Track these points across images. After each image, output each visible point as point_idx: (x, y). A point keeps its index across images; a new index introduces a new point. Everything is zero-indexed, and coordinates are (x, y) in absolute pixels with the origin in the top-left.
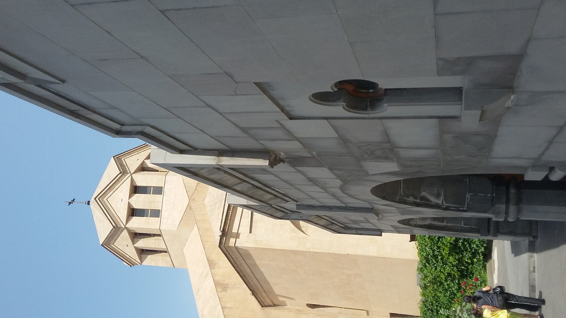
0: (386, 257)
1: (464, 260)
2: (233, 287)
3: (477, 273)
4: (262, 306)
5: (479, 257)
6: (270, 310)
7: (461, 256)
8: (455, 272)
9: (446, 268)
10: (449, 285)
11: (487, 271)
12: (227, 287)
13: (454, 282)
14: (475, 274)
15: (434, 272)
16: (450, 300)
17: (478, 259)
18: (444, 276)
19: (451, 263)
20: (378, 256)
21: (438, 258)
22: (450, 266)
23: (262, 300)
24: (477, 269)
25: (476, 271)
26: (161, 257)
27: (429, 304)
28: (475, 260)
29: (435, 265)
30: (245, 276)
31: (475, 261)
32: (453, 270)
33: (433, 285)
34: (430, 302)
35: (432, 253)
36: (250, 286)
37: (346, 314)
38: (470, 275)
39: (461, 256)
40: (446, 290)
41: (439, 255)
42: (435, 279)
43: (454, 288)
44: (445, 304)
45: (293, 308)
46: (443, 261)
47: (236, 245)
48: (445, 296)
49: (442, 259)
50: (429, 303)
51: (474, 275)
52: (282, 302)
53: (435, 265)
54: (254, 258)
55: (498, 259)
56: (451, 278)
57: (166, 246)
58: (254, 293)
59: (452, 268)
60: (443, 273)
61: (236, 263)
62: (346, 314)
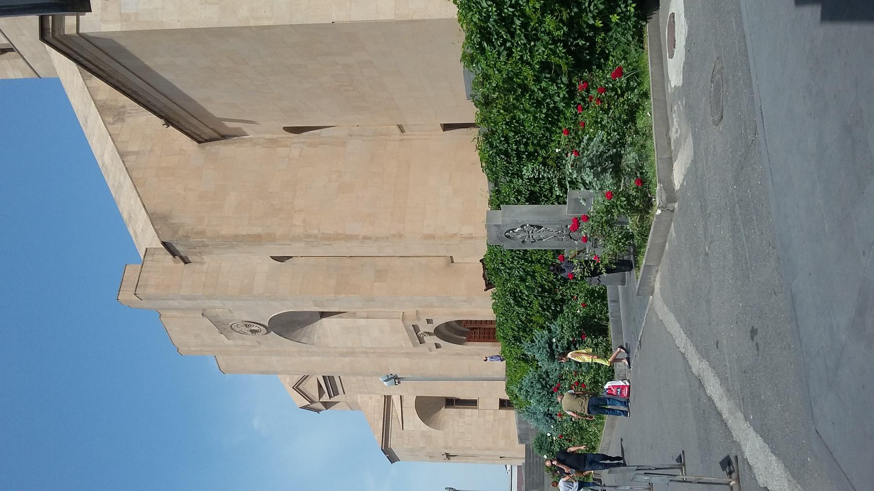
0: (415, 18)
1: (585, 22)
2: (137, 110)
3: (618, 53)
4: (199, 142)
5: (626, 7)
6: (216, 146)
7: (575, 10)
8: (561, 58)
9: (537, 51)
10: (547, 91)
11: (647, 46)
12: (124, 113)
13: (559, 81)
14: (613, 56)
15: (506, 63)
16: (549, 126)
17: (622, 12)
18: (531, 72)
19: (549, 33)
20: (396, 19)
21: (514, 23)
22: (548, 43)
23: (194, 130)
24: (619, 42)
25: (614, 49)
26: (6, 60)
27: (498, 141)
28: (615, 18)
29: (508, 44)
30: (135, 92)
31: (613, 20)
32: (554, 53)
33: (505, 95)
34: (501, 135)
35: (495, 11)
36: (156, 110)
37: (362, 135)
38: (600, 60)
39: (575, 10)
40: (539, 104)
41: (515, 16)
42: (509, 79)
43: (559, 96)
44: (536, 137)
45: (260, 138)
46: (526, 30)
47: (81, 31)
48: (535, 118)
49: (524, 26)
50: (499, 138)
51: (611, 58)
52: (236, 129)
53: (508, 44)
54: (137, 54)
55: (685, 12)
56: (550, 73)
57: (7, 38)
58: (169, 122)
59: (552, 47)
60: (528, 63)
61: (102, 70)
62: (362, 135)
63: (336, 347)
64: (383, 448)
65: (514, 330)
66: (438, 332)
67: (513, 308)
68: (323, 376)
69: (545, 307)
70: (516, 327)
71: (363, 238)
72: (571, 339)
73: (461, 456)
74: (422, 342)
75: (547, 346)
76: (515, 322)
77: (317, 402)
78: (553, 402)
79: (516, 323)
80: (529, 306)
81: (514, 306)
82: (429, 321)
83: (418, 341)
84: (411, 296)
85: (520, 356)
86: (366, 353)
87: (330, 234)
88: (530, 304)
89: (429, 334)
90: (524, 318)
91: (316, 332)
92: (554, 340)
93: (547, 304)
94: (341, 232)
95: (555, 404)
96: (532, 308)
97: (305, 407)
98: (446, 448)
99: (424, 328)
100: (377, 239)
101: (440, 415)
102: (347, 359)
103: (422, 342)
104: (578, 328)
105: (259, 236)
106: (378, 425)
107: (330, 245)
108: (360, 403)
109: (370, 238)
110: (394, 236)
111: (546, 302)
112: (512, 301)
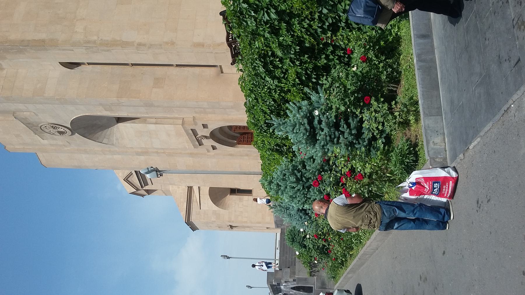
63: (132, 148)
64: (186, 222)
65: (265, 113)
66: (213, 135)
67: (264, 80)
68: (135, 171)
69: (304, 78)
70: (268, 108)
71: (138, 45)
72: (343, 108)
73: (240, 227)
74: (200, 144)
75: (306, 121)
76: (266, 102)
77: (141, 190)
78: (310, 198)
79: (268, 103)
80: (284, 77)
81: (265, 77)
82: (205, 126)
83: (197, 143)
84: (185, 101)
85: (273, 147)
86: (157, 153)
87: (108, 40)
88: (285, 74)
89: (206, 137)
90: (277, 96)
91: (114, 135)
92: (317, 113)
93: (306, 74)
94: (119, 39)
95: (311, 201)
96: (286, 79)
97: (133, 193)
98: (229, 222)
99: (201, 132)
100: (151, 46)
101: (226, 199)
102: (142, 158)
103: (200, 144)
104: (353, 93)
105: (43, 41)
106: (183, 206)
107: (108, 51)
108: (171, 191)
109: (144, 45)
110: (167, 43)
111: (306, 72)
112: (262, 69)
